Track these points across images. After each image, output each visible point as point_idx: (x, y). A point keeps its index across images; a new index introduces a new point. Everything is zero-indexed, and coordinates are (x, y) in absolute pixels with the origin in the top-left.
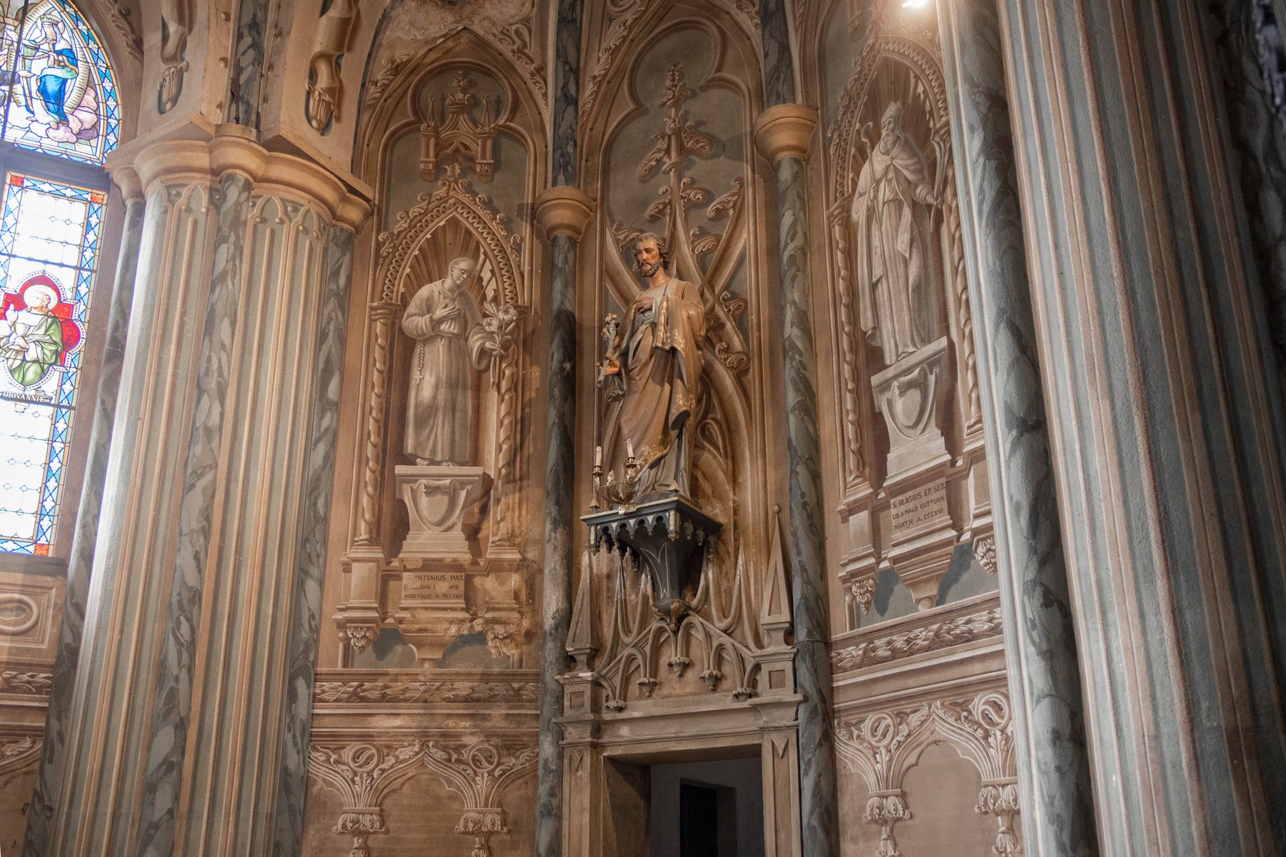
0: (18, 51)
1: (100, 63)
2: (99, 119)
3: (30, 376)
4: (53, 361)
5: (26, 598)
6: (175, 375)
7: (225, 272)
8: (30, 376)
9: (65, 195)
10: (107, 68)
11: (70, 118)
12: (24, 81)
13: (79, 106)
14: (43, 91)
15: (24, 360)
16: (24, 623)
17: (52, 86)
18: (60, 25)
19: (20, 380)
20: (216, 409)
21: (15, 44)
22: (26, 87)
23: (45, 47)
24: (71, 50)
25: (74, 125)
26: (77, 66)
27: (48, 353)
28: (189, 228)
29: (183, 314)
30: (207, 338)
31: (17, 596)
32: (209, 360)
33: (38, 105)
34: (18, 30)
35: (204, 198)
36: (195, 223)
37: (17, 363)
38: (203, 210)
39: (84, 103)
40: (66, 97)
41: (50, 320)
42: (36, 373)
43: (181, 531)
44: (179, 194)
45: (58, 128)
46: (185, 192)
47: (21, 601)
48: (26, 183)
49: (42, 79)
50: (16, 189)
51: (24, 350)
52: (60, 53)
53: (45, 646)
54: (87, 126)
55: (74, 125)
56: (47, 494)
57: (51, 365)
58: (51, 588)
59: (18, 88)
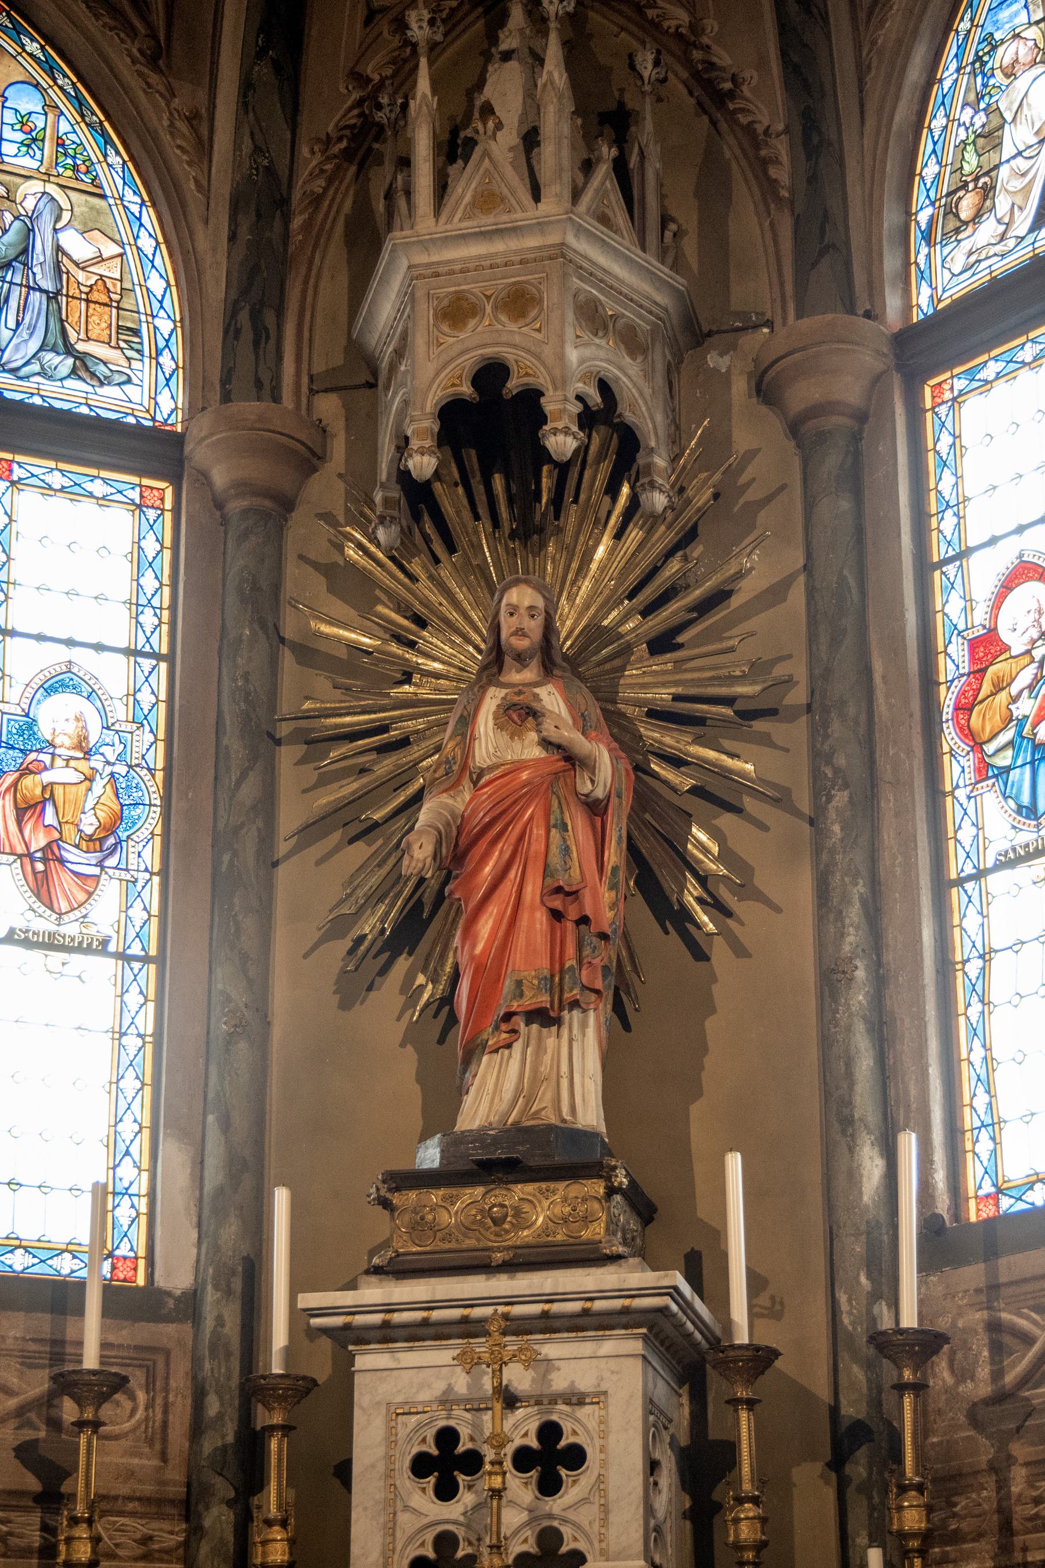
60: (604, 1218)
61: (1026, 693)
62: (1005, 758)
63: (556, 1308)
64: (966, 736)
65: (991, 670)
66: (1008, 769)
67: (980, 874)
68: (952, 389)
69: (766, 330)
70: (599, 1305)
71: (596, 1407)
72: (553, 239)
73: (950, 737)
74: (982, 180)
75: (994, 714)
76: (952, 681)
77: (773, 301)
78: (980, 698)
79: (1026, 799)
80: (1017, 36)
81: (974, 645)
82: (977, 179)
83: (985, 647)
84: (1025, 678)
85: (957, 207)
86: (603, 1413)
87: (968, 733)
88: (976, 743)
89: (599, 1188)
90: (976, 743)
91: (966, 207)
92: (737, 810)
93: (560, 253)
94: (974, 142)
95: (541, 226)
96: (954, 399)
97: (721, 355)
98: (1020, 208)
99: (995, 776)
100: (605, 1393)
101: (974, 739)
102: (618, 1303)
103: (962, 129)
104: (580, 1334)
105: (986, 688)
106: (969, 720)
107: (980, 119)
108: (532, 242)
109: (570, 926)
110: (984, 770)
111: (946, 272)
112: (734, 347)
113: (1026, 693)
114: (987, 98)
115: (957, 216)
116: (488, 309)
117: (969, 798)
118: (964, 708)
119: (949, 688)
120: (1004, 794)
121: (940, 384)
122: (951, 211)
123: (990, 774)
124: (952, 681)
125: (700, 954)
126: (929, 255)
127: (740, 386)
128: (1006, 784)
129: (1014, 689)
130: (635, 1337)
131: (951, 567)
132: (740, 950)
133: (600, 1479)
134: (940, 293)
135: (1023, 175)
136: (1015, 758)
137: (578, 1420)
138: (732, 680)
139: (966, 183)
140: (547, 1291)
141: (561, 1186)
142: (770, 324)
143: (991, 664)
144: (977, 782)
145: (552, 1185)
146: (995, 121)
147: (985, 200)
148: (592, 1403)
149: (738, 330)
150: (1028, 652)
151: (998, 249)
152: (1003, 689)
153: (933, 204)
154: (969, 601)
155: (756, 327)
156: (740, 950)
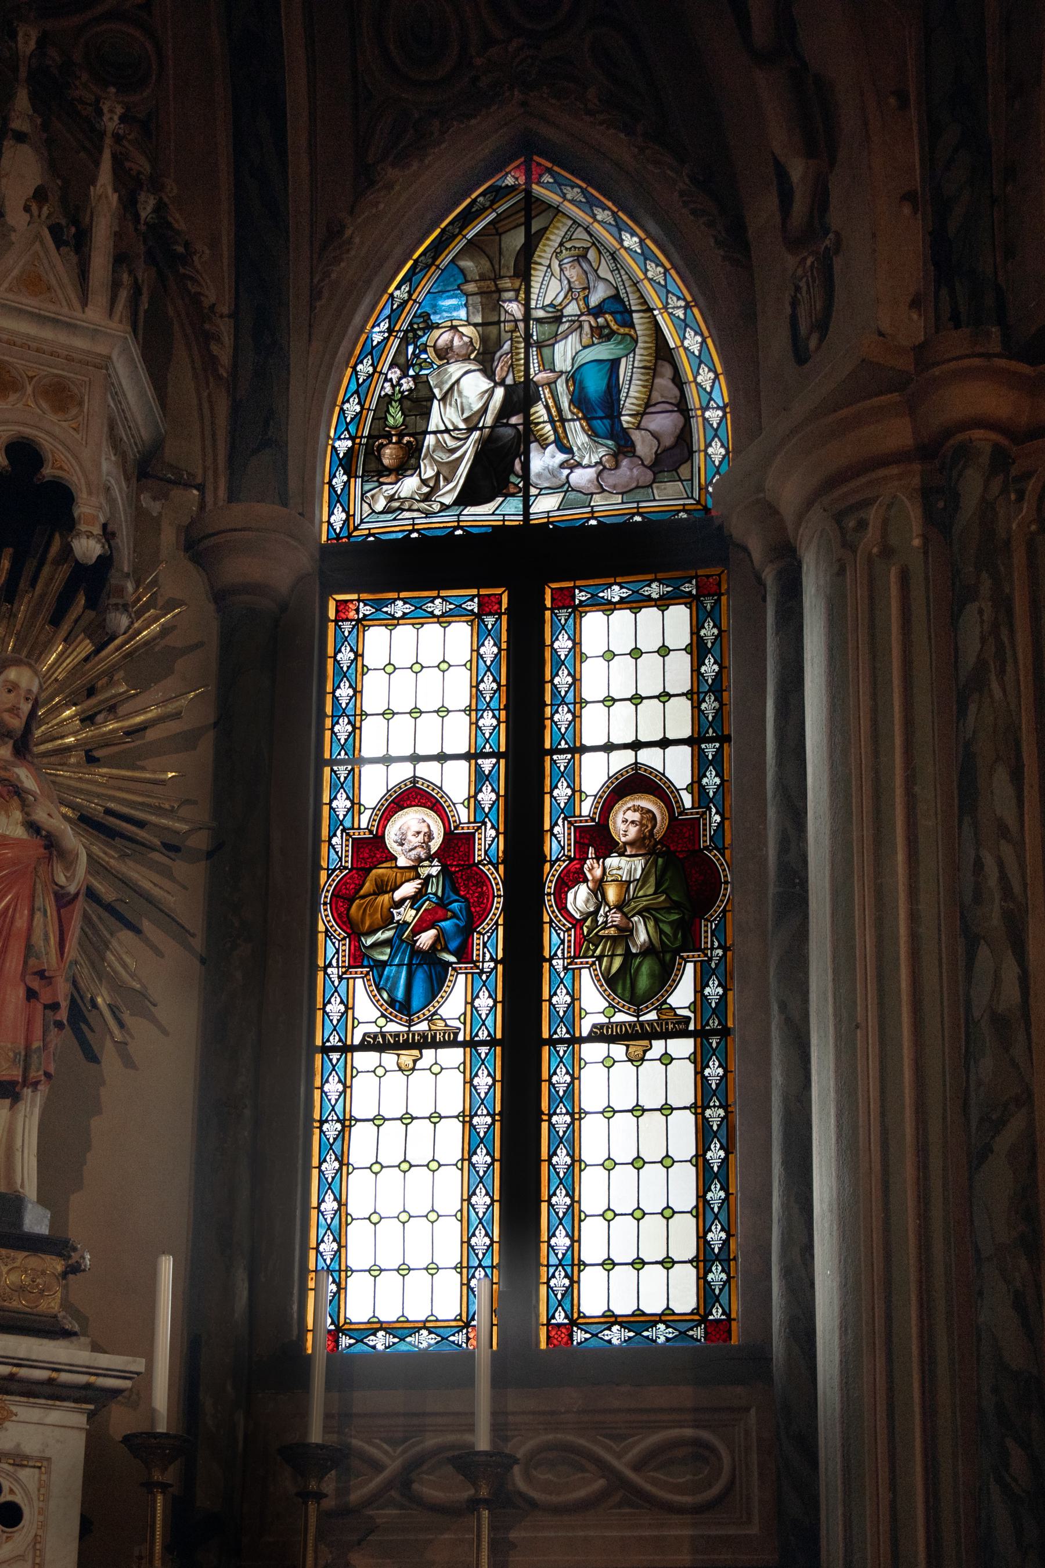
0: (528, 335)
1: (673, 301)
2: (687, 419)
3: (643, 982)
4: (677, 944)
5: (705, 1435)
6: (914, 917)
7: (982, 664)
8: (643, 982)
9: (649, 598)
10: (687, 306)
11: (636, 436)
12: (545, 393)
13: (647, 405)
14: (579, 400)
15: (628, 956)
16: (710, 1486)
17: (595, 384)
18: (592, 255)
19: (627, 994)
20: (1010, 970)
21: (521, 325)
22: (551, 403)
23: (572, 309)
24: (616, 297)
25: (645, 446)
26: (632, 326)
27: (667, 929)
28: (894, 591)
29: (910, 781)
30: (967, 819)
31: (688, 1432)
32: (979, 865)
33: (578, 435)
34: (522, 295)
35: (914, 514)
36: (904, 577)
37: (617, 962)
38: (916, 542)
39: (656, 396)
40: (623, 394)
41: (660, 861)
42: (652, 975)
43: (978, 1251)
44: (862, 525)
45: (617, 466)
46: (873, 515)
47: (697, 1443)
48: (580, 596)
49: (574, 377)
50: (563, 614)
51: (626, 933)
52: (597, 311)
53: (754, 1530)
54: (668, 441)
55: (645, 446)
56: (710, 1217)
57: (676, 952)
58: (747, 1409)
59: (539, 411)
60: (59, 1294)
61: (408, 903)
62: (383, 954)
63: (23, 1372)
64: (344, 923)
65: (374, 871)
66: (384, 964)
67: (346, 1049)
68: (357, 611)
69: (195, 492)
70: (64, 1377)
71: (37, 1471)
72: (101, 349)
73: (325, 919)
74: (406, 439)
75: (376, 911)
76: (334, 870)
77: (205, 469)
78: (362, 892)
79: (400, 994)
80: (454, 328)
81: (358, 844)
82: (401, 436)
83: (370, 851)
84: (408, 889)
85: (379, 451)
86: (44, 1477)
87: (344, 920)
88: (354, 932)
89: (59, 1266)
90: (354, 932)
91: (389, 455)
92: (137, 931)
93: (104, 363)
94: (400, 401)
95: (95, 333)
96: (359, 621)
97: (154, 499)
98: (446, 479)
99: (371, 968)
100: (49, 1459)
101: (352, 928)
102: (83, 1379)
103: (387, 385)
104: (32, 1400)
105: (368, 887)
106: (349, 909)
107: (407, 384)
108: (80, 343)
109: (40, 1007)
110: (359, 958)
111: (366, 507)
112: (166, 497)
113: (408, 903)
114: (417, 368)
115: (379, 459)
116: (29, 389)
117: (340, 978)
118: (344, 897)
119: (329, 876)
120: (377, 986)
121: (346, 602)
122: (373, 454)
123: (366, 963)
124: (334, 870)
125: (92, 1057)
126: (347, 484)
127: (168, 537)
128: (381, 976)
129: (398, 895)
130: (81, 1411)
131: (342, 768)
132: (128, 1061)
133: (36, 1540)
134: (358, 521)
135: (453, 451)
136: (392, 956)
137: (17, 1480)
138: (159, 810)
139: (389, 436)
140: (21, 1356)
141: (20, 1255)
142: (201, 488)
143: (375, 867)
144: (350, 967)
145: (12, 1253)
146: (423, 393)
147: (410, 458)
148: (34, 1467)
149: (169, 481)
150: (414, 868)
151: (423, 505)
152: (387, 892)
153: (352, 438)
154: (355, 805)
155: (188, 486)
156: (128, 1061)
